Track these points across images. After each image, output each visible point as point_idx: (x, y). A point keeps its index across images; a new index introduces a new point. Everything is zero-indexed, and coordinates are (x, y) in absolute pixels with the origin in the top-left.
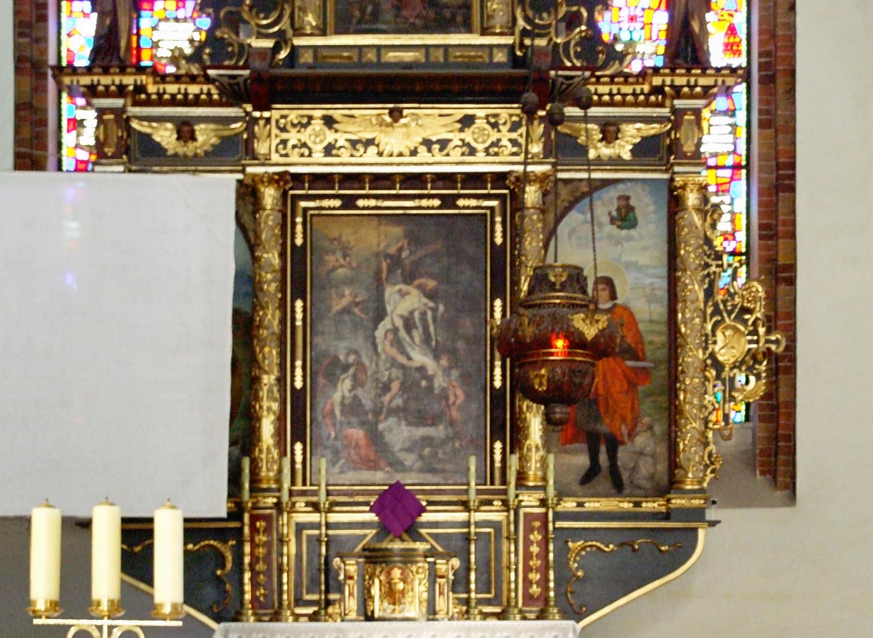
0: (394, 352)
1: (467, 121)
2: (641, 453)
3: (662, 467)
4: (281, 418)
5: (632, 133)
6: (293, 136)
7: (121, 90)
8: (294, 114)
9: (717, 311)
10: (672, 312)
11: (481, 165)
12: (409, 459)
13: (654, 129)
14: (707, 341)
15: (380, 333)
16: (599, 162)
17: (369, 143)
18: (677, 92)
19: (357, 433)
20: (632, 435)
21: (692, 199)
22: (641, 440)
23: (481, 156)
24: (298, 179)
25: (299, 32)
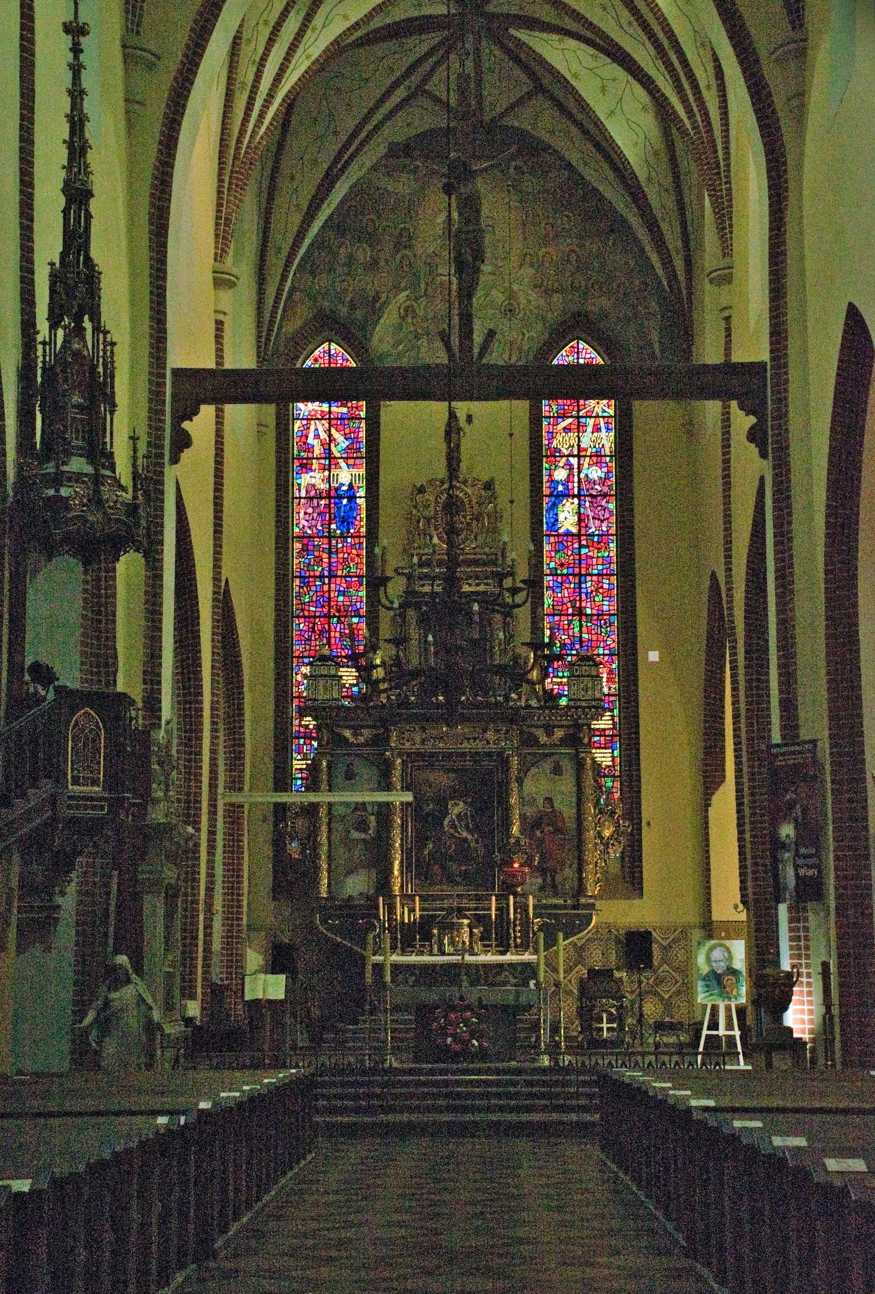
0: (452, 831)
4: (402, 862)
9: (601, 812)
22: (567, 872)
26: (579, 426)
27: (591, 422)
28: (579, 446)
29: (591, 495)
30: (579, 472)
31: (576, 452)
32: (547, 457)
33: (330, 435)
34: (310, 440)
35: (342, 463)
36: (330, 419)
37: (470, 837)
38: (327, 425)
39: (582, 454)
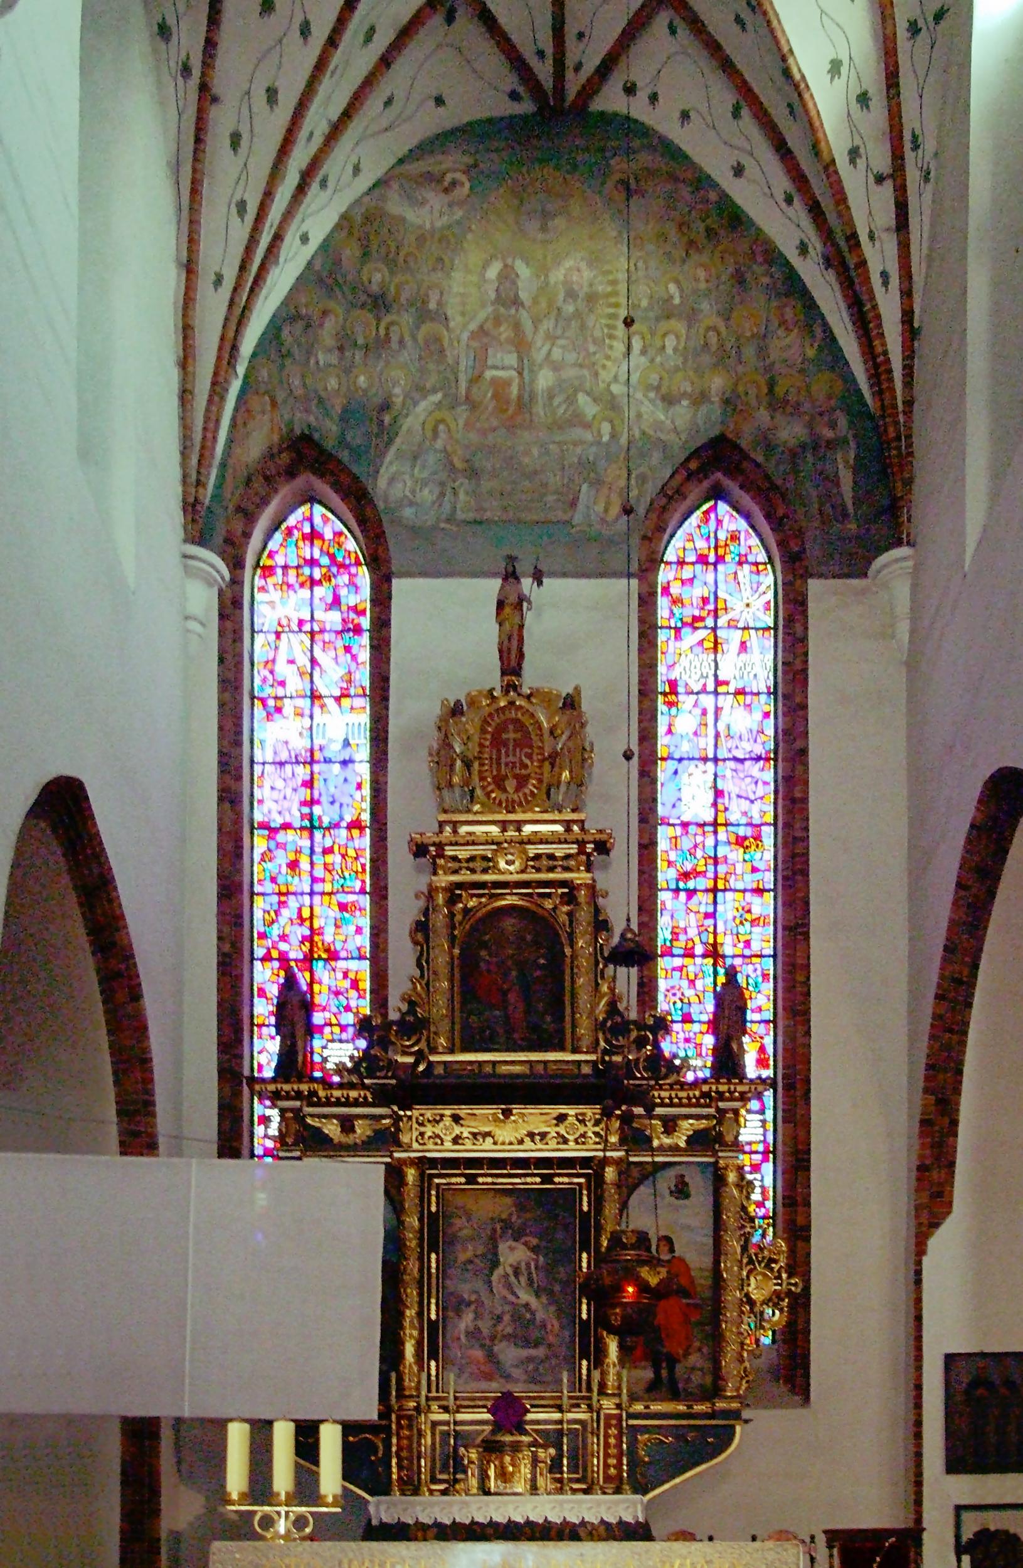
1: (561, 1118)
2: (693, 1369)
3: (709, 1380)
4: (419, 1344)
5: (687, 1127)
6: (429, 1130)
7: (299, 1095)
8: (429, 1114)
9: (751, 1262)
10: (717, 1262)
11: (571, 1152)
12: (516, 1373)
13: (703, 1124)
14: (743, 1283)
15: (495, 1278)
16: (662, 1149)
17: (488, 1134)
18: (721, 1096)
19: (478, 1354)
20: (687, 1354)
21: (732, 1177)
22: (694, 1359)
23: (572, 1144)
24: (433, 1163)
25: (433, 1050)
26: (716, 643)
27: (736, 637)
28: (716, 676)
29: (735, 759)
30: (716, 720)
31: (711, 687)
32: (665, 694)
33: (314, 662)
34: (282, 669)
35: (330, 703)
36: (312, 634)
37: (534, 1302)
38: (308, 643)
39: (721, 689)
